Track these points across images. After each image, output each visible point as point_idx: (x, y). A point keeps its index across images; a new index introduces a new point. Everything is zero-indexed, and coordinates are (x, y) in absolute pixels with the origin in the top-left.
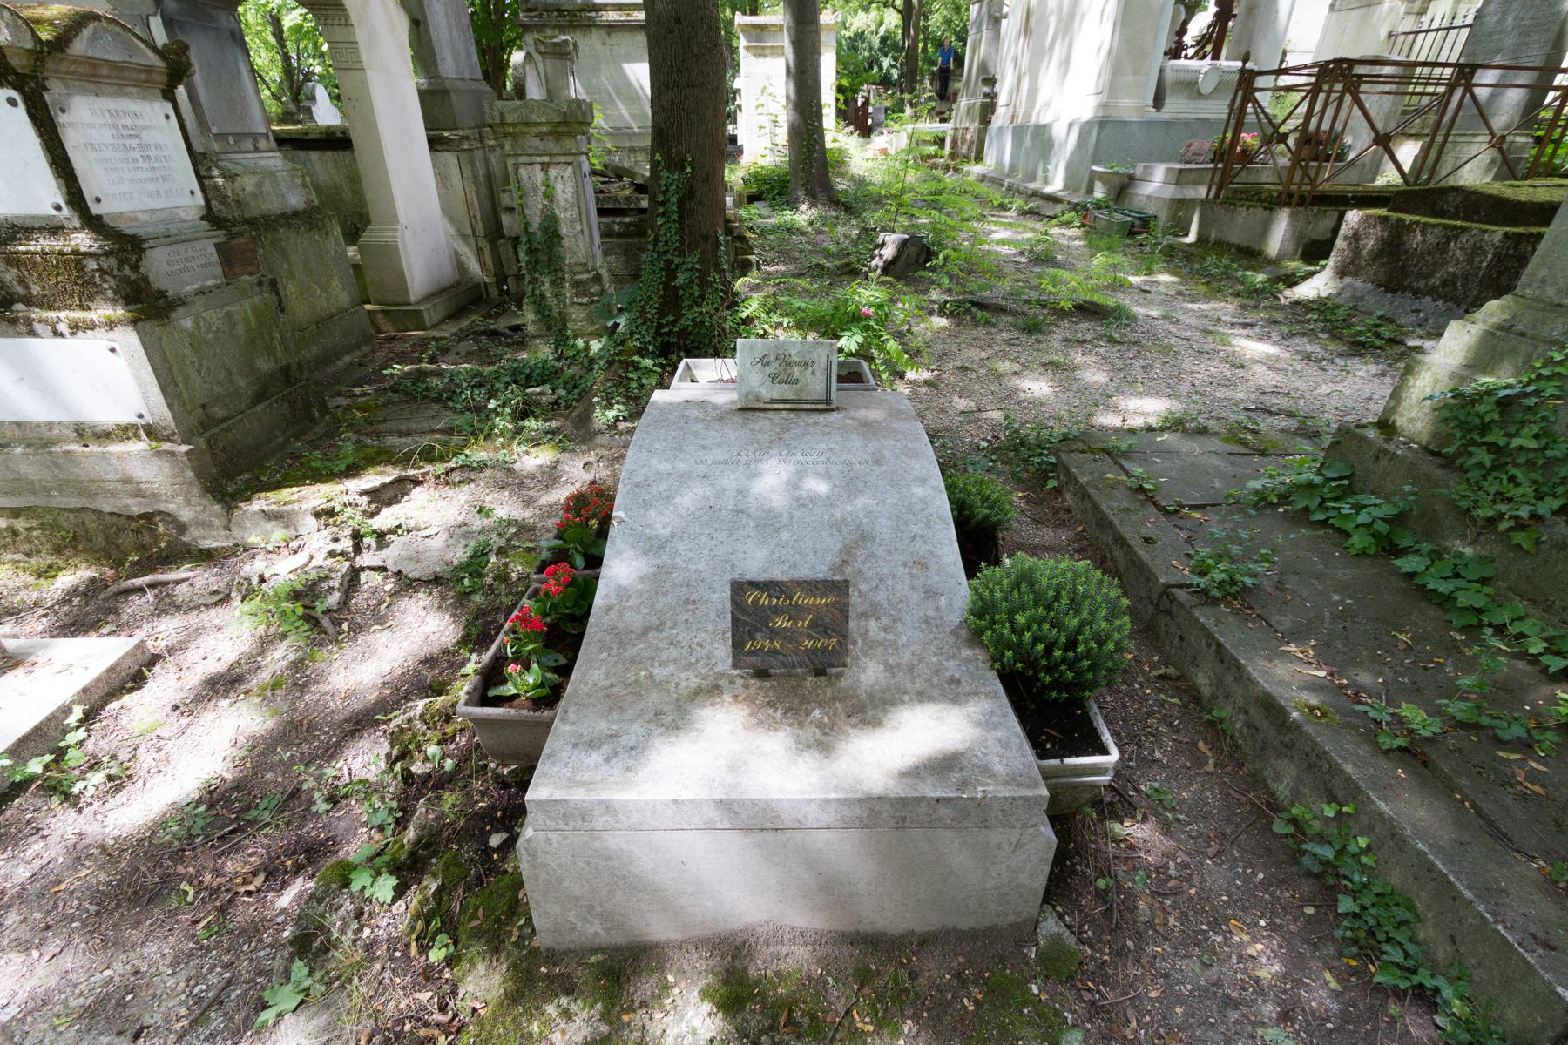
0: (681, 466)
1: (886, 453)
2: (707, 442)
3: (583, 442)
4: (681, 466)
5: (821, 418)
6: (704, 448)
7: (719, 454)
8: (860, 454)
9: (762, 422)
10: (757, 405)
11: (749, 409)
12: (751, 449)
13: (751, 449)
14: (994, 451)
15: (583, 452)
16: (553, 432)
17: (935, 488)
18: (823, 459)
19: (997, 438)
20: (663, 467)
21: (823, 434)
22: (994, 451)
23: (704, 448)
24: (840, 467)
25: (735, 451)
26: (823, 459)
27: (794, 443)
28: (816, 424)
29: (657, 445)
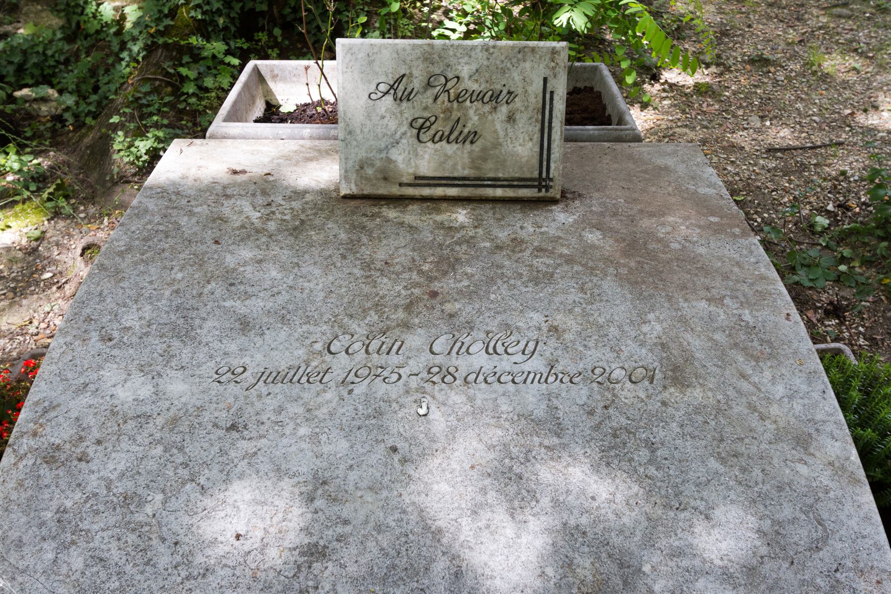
0: (178, 387)
1: (695, 343)
2: (255, 307)
3: (91, 199)
4: (178, 387)
5: (527, 226)
6: (245, 325)
7: (281, 349)
8: (630, 347)
9: (398, 240)
10: (382, 191)
11: (372, 198)
12: (359, 328)
13: (359, 328)
14: (843, 238)
15: (90, 219)
16: (40, 179)
17: (837, 468)
18: (537, 364)
19: (844, 207)
20: (128, 390)
21: (539, 279)
22: (843, 238)
23: (245, 325)
24: (582, 393)
25: (321, 332)
26: (537, 364)
27: (465, 309)
28: (517, 243)
29: (130, 319)
